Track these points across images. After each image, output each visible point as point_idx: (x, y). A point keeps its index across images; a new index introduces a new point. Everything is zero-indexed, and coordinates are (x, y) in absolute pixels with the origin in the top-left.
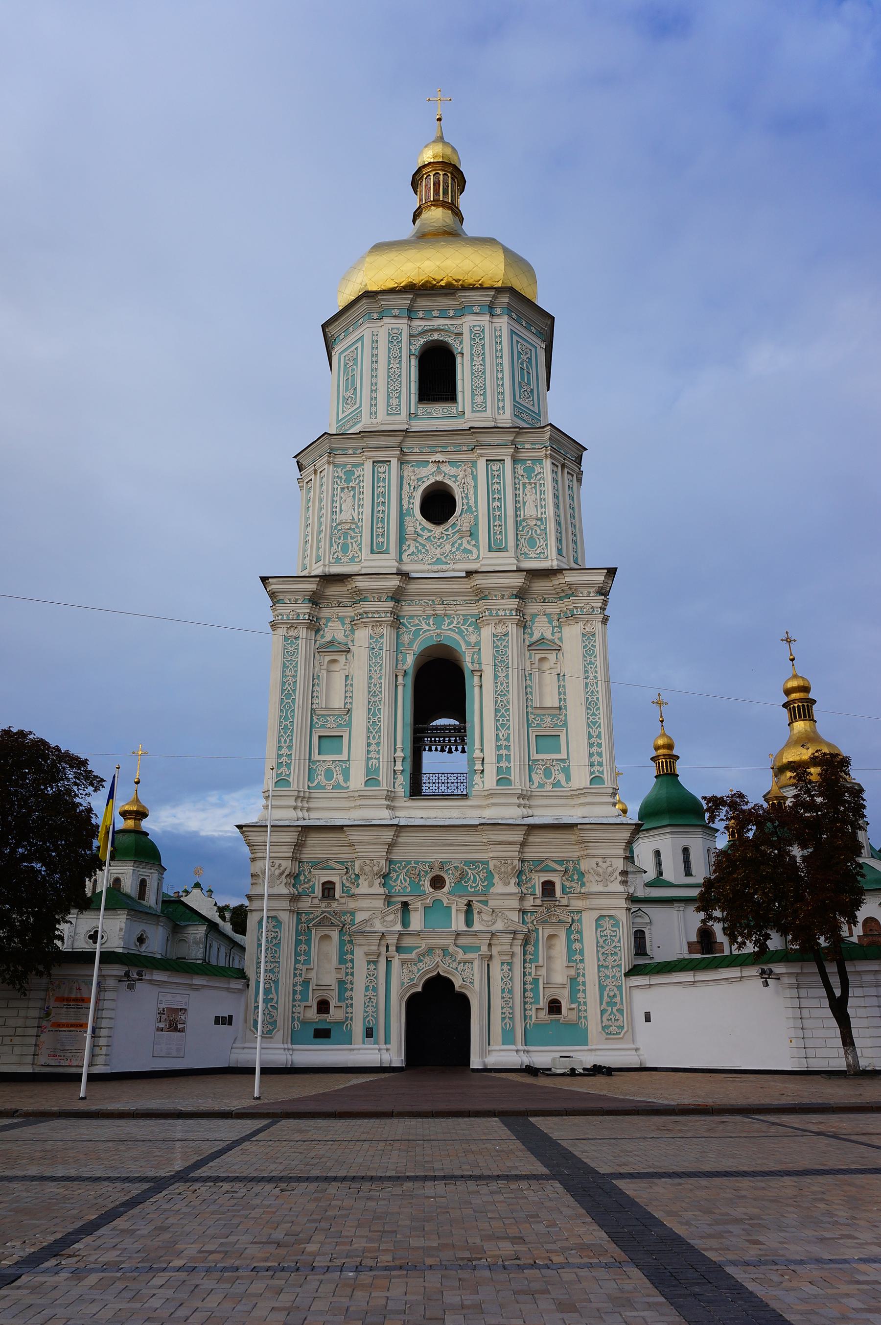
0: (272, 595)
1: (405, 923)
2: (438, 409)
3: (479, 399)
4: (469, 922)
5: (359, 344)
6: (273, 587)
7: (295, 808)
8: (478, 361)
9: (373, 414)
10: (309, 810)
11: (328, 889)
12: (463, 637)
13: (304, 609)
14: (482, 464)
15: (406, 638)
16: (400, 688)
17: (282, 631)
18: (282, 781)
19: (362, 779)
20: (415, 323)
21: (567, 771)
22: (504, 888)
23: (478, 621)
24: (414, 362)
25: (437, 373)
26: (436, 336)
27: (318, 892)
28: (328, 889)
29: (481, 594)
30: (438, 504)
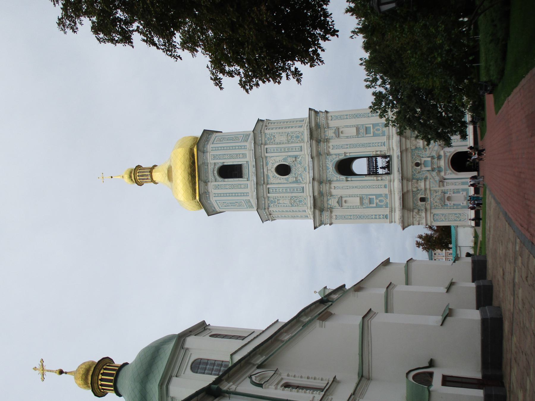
0: (320, 225)
2: (245, 171)
3: (241, 156)
5: (218, 202)
6: (317, 225)
7: (395, 212)
8: (226, 157)
10: (395, 208)
12: (333, 159)
13: (326, 214)
16: (352, 179)
17: (333, 221)
18: (386, 217)
23: (328, 154)
24: (226, 180)
25: (230, 172)
26: (216, 172)
27: (423, 203)
29: (319, 154)
30: (283, 170)
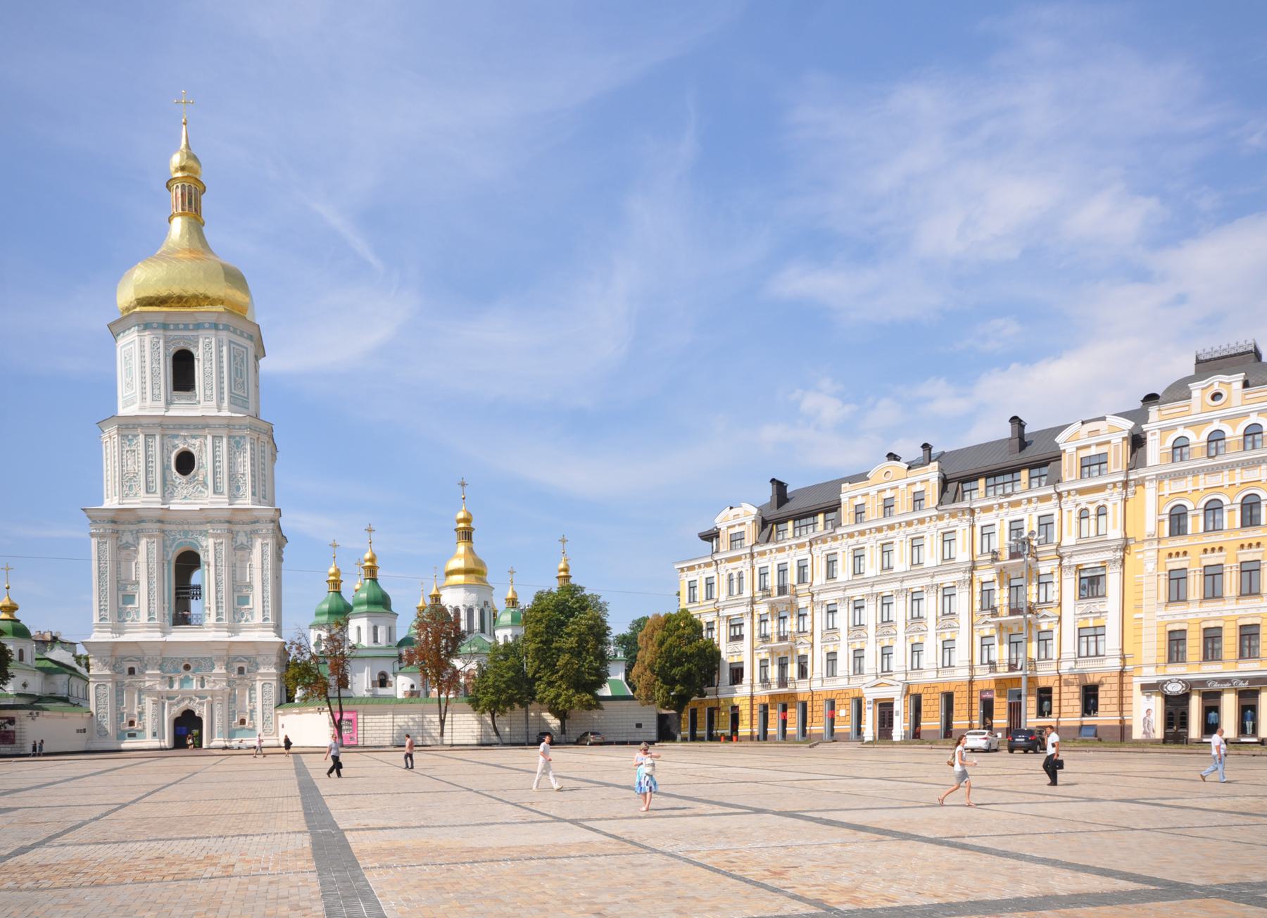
1: (171, 686)
4: (202, 686)
8: (208, 365)
9: (144, 399)
11: (132, 671)
13: (109, 526)
14: (209, 438)
15: (168, 543)
19: (146, 617)
20: (169, 333)
21: (252, 614)
22: (219, 670)
25: (182, 371)
26: (182, 346)
28: (132, 671)
